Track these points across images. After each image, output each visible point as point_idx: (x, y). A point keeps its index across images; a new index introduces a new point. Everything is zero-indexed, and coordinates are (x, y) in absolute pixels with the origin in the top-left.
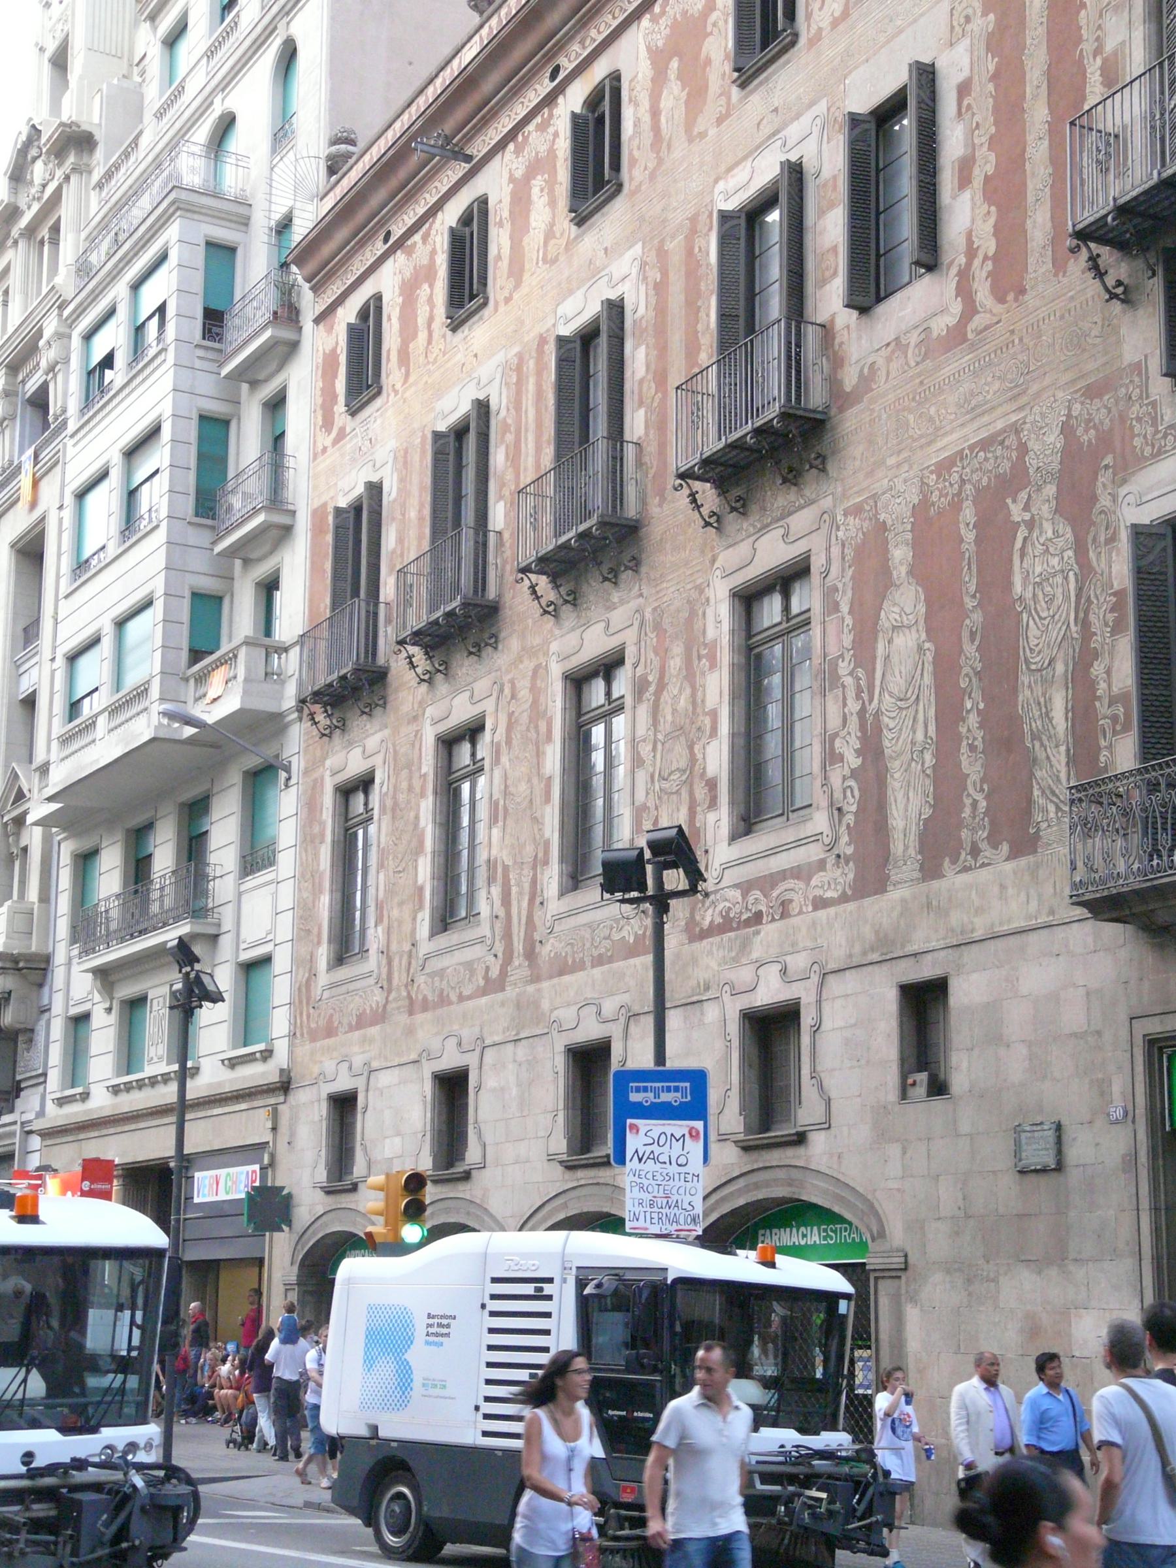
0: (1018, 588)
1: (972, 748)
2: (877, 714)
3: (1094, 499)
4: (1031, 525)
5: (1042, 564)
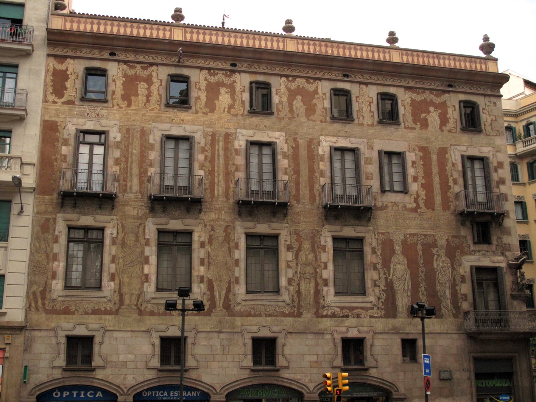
1: (423, 294)
2: (392, 280)
3: (455, 257)
5: (441, 263)
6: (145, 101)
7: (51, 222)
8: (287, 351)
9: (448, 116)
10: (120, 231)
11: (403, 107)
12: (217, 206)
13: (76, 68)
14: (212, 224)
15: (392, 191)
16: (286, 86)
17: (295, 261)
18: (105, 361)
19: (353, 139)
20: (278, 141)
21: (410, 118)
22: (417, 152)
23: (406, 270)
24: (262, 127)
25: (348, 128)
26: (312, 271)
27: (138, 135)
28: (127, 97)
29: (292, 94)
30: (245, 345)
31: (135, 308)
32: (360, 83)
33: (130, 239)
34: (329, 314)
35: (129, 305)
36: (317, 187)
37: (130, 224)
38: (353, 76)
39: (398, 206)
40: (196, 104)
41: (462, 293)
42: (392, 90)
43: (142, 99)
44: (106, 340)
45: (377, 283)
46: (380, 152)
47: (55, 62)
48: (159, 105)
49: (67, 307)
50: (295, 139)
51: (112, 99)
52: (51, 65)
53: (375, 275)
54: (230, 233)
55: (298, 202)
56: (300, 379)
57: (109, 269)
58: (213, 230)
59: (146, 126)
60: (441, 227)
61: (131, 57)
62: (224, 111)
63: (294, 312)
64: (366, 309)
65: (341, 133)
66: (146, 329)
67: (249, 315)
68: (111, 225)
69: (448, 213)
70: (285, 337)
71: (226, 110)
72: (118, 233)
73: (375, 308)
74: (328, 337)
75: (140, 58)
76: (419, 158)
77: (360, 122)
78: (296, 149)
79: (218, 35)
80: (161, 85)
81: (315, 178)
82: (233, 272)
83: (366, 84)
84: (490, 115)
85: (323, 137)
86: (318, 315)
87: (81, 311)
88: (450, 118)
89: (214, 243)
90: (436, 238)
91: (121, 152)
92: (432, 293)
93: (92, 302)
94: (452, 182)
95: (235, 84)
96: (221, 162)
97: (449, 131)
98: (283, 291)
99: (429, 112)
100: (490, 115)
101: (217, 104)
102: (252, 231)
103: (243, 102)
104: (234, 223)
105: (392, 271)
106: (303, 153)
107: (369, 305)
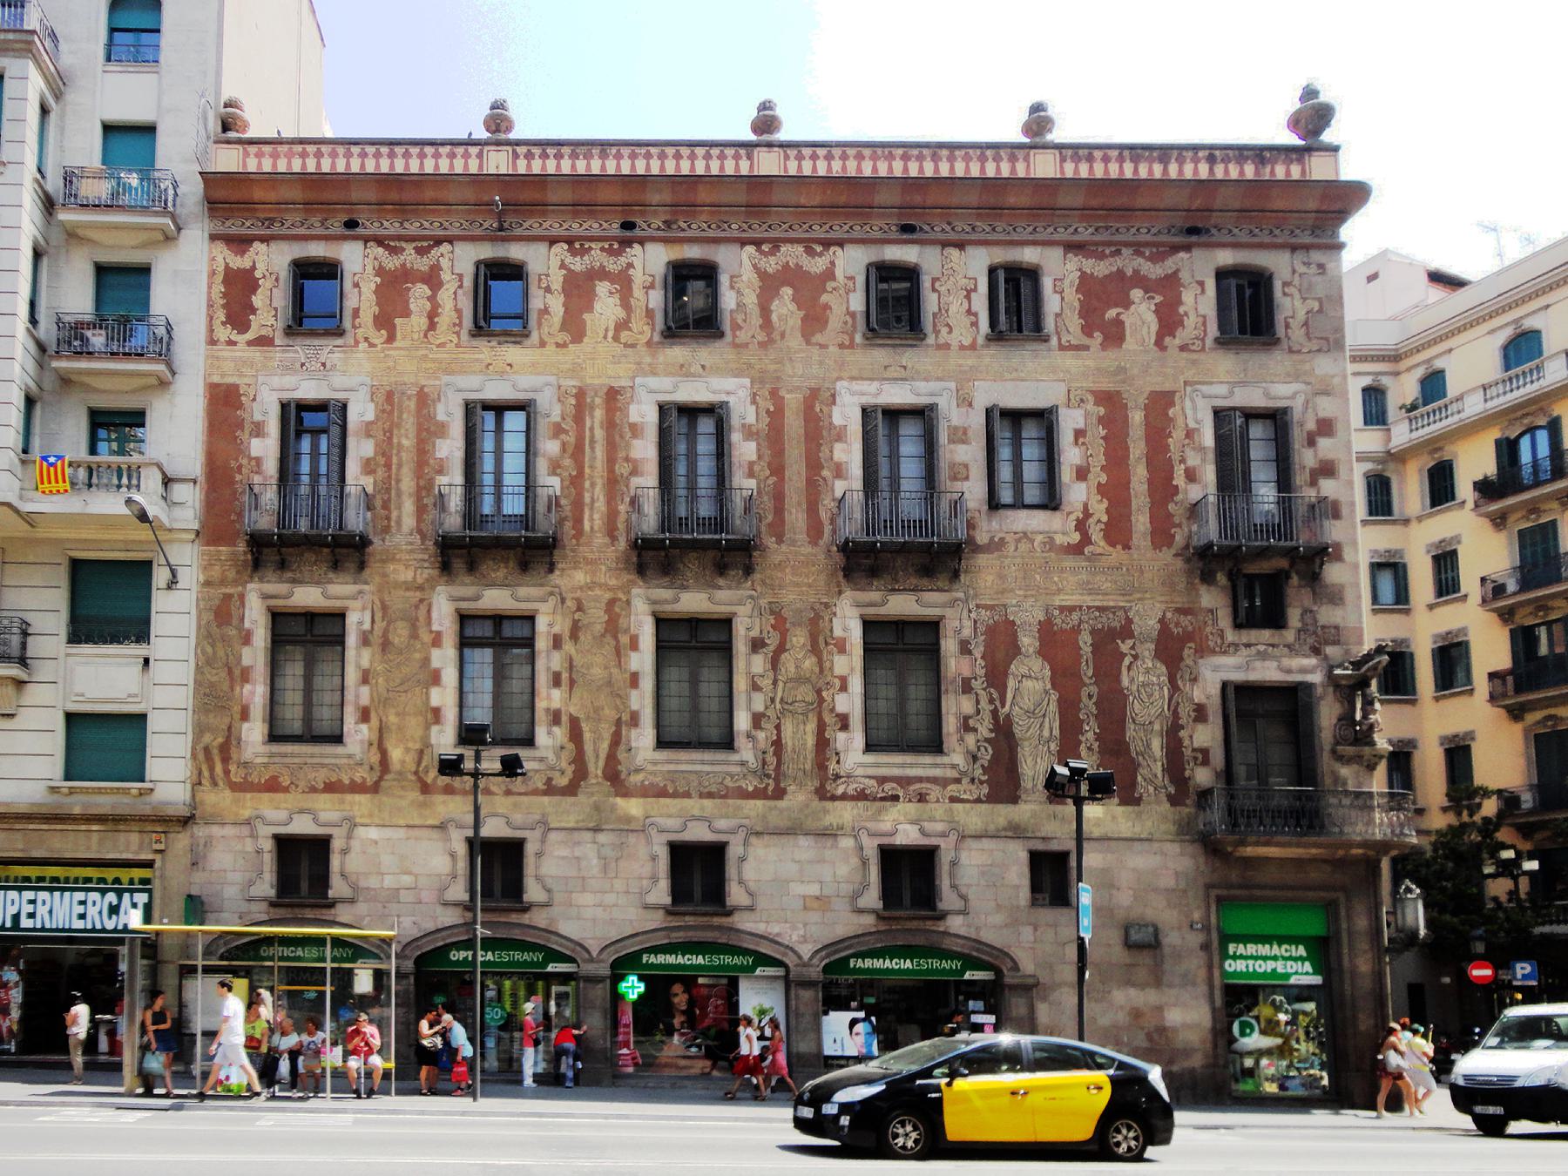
0: (1125, 682)
1: (1089, 749)
3: (1182, 659)
4: (1136, 657)
5: (1143, 677)
6: (425, 327)
7: (236, 602)
8: (750, 872)
9: (1181, 310)
10: (378, 616)
11: (1058, 297)
12: (590, 556)
13: (272, 261)
14: (579, 594)
15: (1019, 504)
16: (755, 266)
17: (771, 674)
18: (355, 887)
19: (922, 386)
20: (732, 400)
21: (1074, 323)
22: (1090, 406)
23: (1046, 692)
24: (696, 368)
25: (909, 357)
26: (811, 696)
27: (412, 404)
28: (385, 321)
29: (769, 286)
30: (654, 858)
31: (413, 778)
32: (945, 244)
33: (400, 634)
34: (850, 791)
35: (400, 773)
36: (826, 506)
37: (400, 600)
38: (926, 228)
39: (1032, 541)
40: (540, 324)
41: (1196, 745)
42: (1029, 255)
43: (418, 321)
44: (355, 844)
45: (971, 722)
46: (989, 412)
47: (227, 252)
48: (458, 334)
49: (274, 778)
50: (774, 393)
51: (354, 327)
52: (220, 259)
53: (967, 706)
54: (619, 616)
55: (780, 541)
56: (778, 935)
57: (357, 696)
58: (580, 608)
59: (430, 383)
60: (1143, 586)
61: (391, 227)
62: (605, 337)
63: (766, 788)
64: (943, 782)
65: (890, 373)
66: (436, 823)
67: (662, 793)
68: (357, 604)
69: (1167, 555)
70: (746, 843)
71: (611, 334)
72: (373, 621)
73: (965, 781)
74: (847, 843)
75: (412, 228)
76: (1095, 421)
77: (941, 341)
78: (776, 416)
79: (592, 157)
80: (461, 287)
81: (821, 482)
82: (624, 699)
83: (960, 246)
84: (1305, 299)
85: (845, 383)
86: (823, 794)
87: (302, 784)
88: (1186, 314)
89: (582, 638)
90: (1131, 615)
91: (376, 445)
92: (1114, 743)
93: (323, 765)
94: (1183, 478)
95: (631, 272)
96: (597, 457)
97: (1183, 348)
98: (741, 742)
99: (1127, 304)
100: (1305, 299)
101: (589, 323)
102: (668, 608)
103: (649, 313)
104: (629, 592)
105: (1009, 696)
106: (794, 424)
107: (951, 774)
